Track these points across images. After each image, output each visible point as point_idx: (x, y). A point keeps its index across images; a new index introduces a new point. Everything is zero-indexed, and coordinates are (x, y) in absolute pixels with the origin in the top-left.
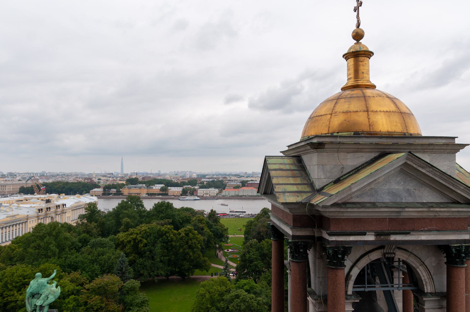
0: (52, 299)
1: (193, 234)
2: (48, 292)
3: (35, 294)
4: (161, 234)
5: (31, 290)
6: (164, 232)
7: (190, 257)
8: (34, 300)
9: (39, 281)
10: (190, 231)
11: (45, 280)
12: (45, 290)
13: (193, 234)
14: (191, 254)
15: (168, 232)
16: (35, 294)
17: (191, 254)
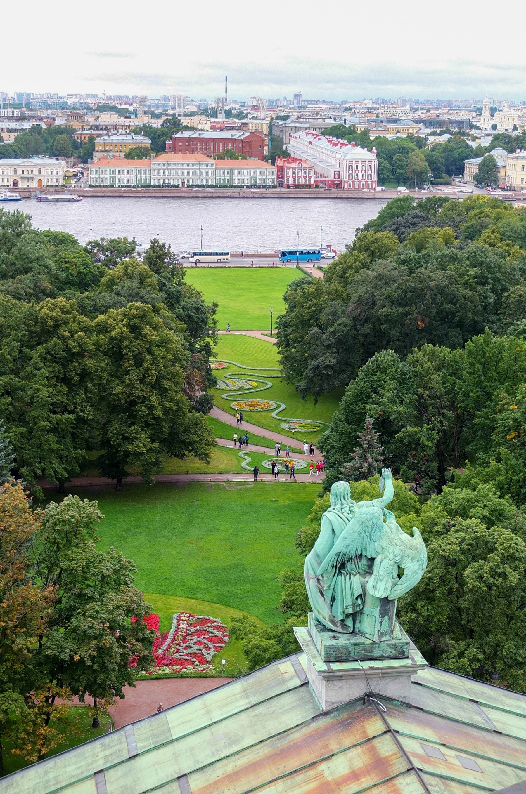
0: (415, 572)
1: (155, 328)
2: (397, 552)
3: (350, 560)
4: (42, 331)
5: (339, 546)
6: (51, 323)
7: (152, 408)
8: (351, 584)
9: (356, 509)
10: (143, 316)
11: (371, 508)
12: (384, 543)
13: (155, 328)
14: (154, 399)
15: (66, 323)
16: (350, 560)
17: (154, 399)
